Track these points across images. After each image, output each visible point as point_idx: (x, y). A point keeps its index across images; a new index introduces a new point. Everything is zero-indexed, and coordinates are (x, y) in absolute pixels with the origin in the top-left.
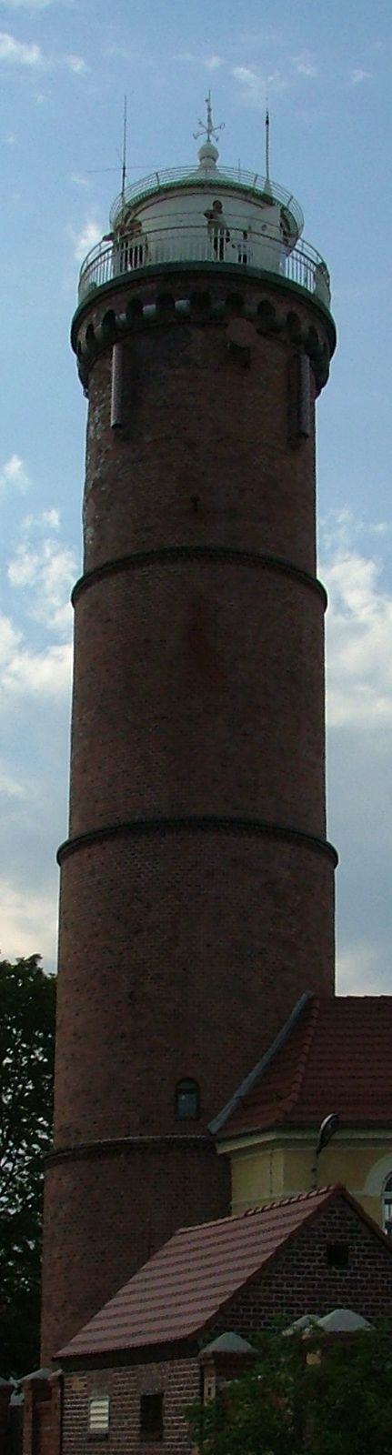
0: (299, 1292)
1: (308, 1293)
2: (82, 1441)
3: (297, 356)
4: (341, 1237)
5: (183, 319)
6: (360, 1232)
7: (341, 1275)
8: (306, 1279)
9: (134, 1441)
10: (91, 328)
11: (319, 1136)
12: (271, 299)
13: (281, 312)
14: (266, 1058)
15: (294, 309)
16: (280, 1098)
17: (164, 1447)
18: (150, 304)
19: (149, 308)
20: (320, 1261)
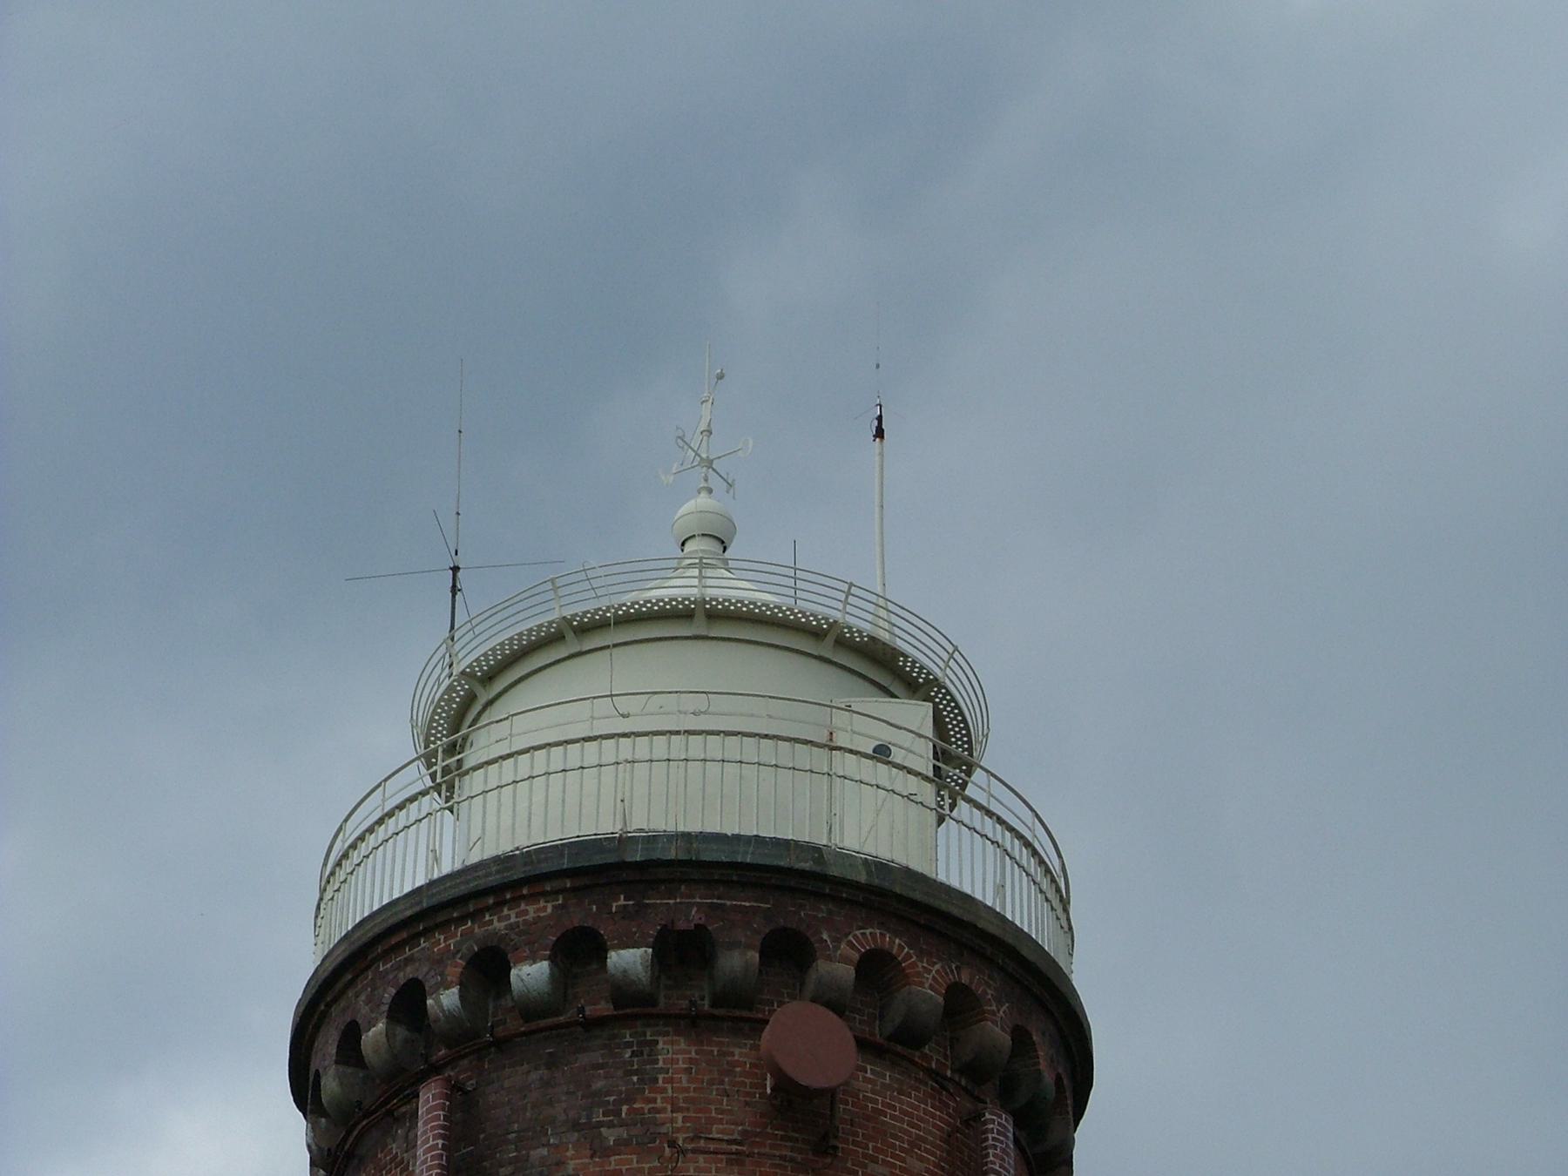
3: (973, 1120)
10: (351, 1035)
15: (965, 979)
18: (534, 959)
19: (531, 974)
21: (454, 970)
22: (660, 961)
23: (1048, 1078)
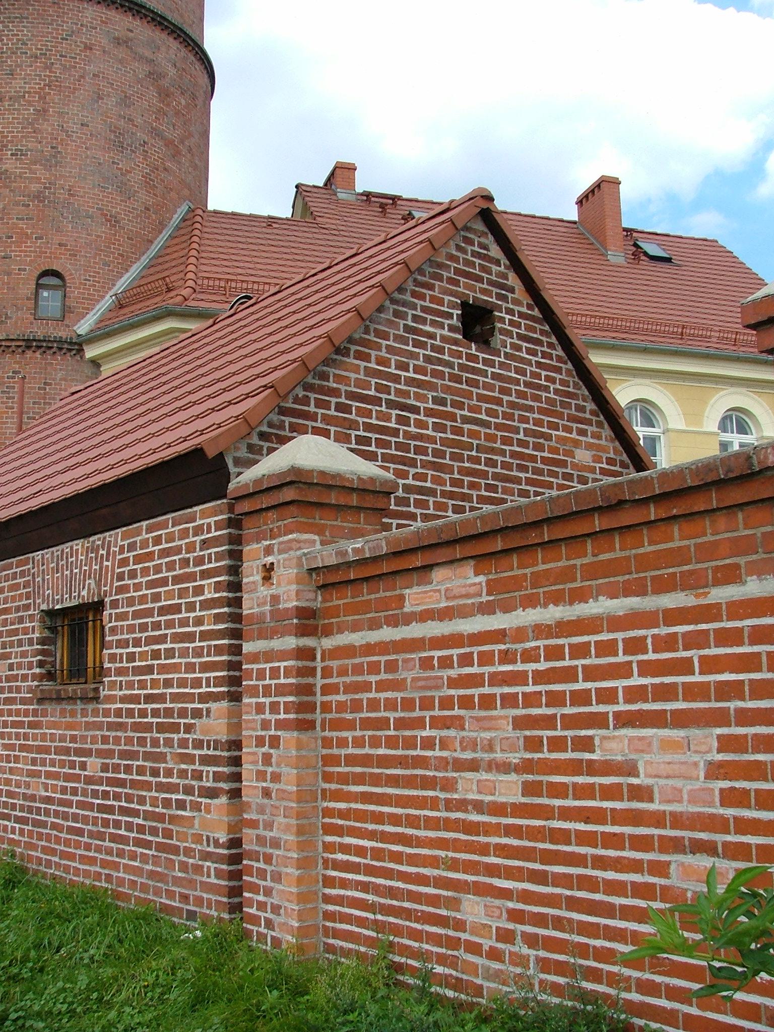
0: (419, 384)
4: (484, 291)
6: (512, 290)
8: (428, 359)
9: (23, 701)
14: (144, 260)
17: (106, 713)
20: (452, 328)
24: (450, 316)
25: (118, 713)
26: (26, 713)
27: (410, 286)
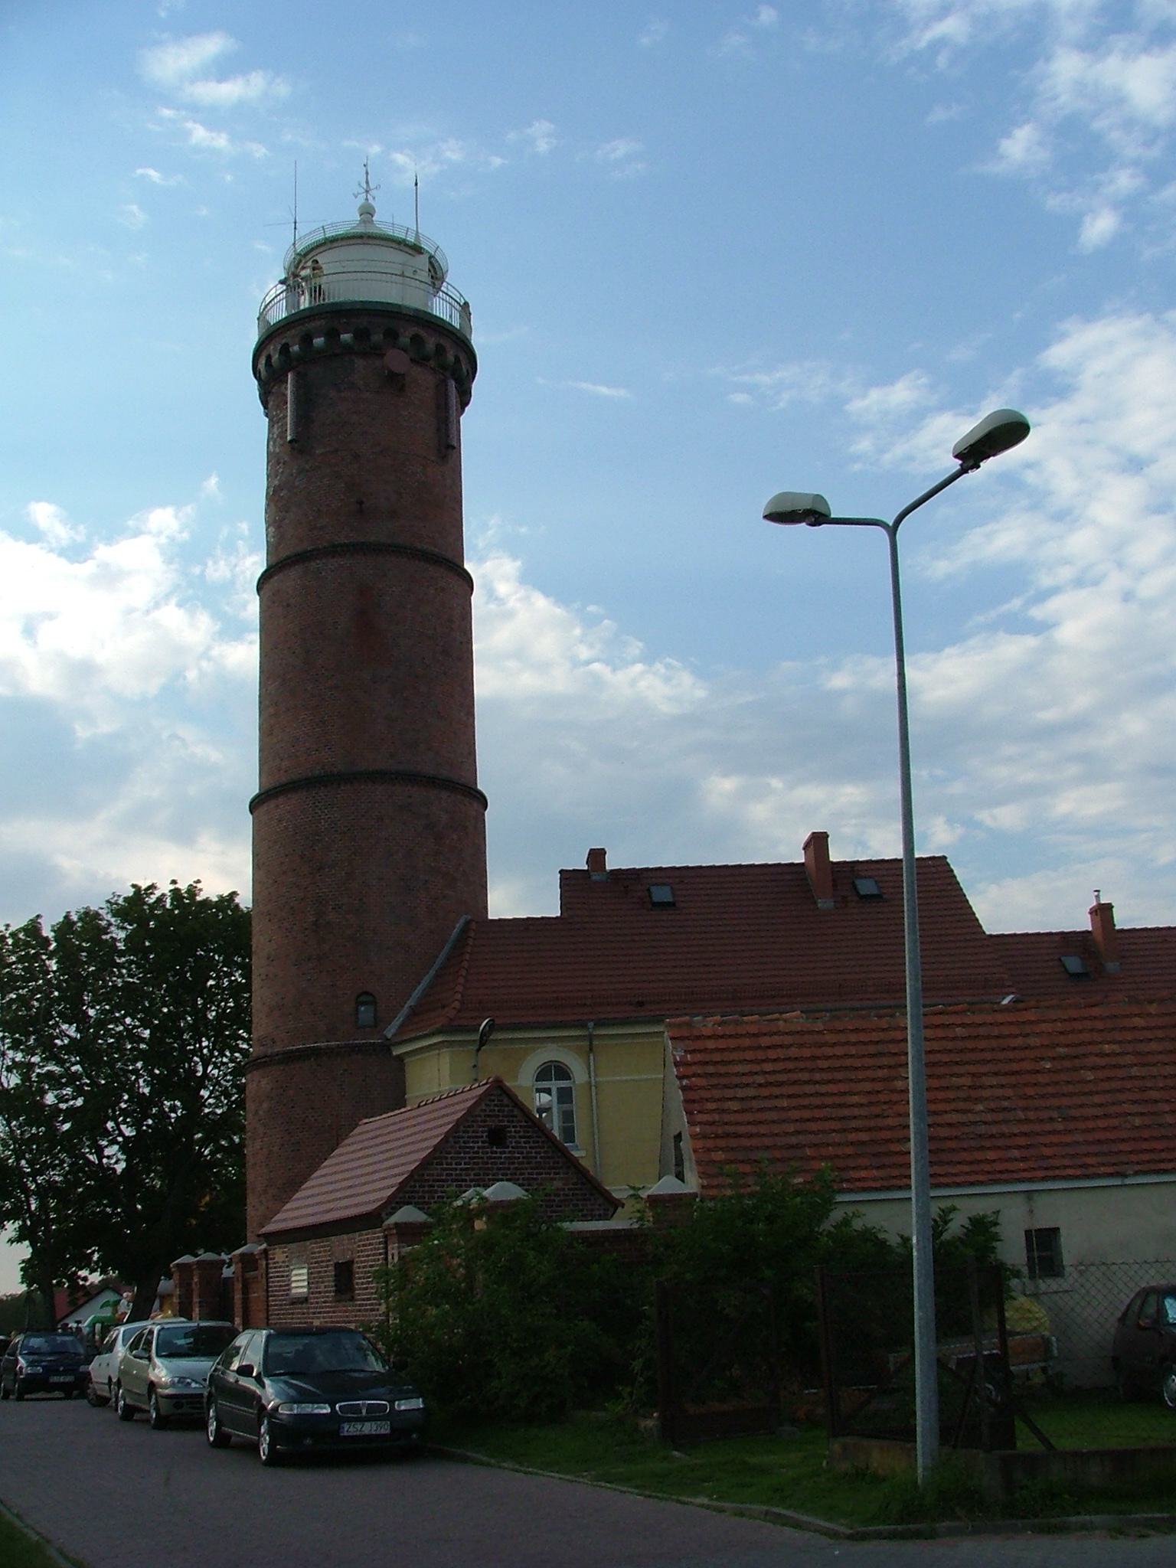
1: (473, 1169)
2: (285, 1305)
5: (348, 349)
6: (516, 1117)
7: (501, 1153)
9: (331, 1302)
10: (269, 358)
11: (476, 1037)
12: (422, 333)
13: (431, 343)
14: (432, 972)
16: (443, 1007)
17: (356, 1305)
18: (320, 337)
19: (319, 341)
20: (482, 1142)
21: (297, 340)
22: (355, 337)
23: (464, 370)
24: (482, 1137)
25: (360, 1305)
26: (331, 1307)
27: (462, 1128)
